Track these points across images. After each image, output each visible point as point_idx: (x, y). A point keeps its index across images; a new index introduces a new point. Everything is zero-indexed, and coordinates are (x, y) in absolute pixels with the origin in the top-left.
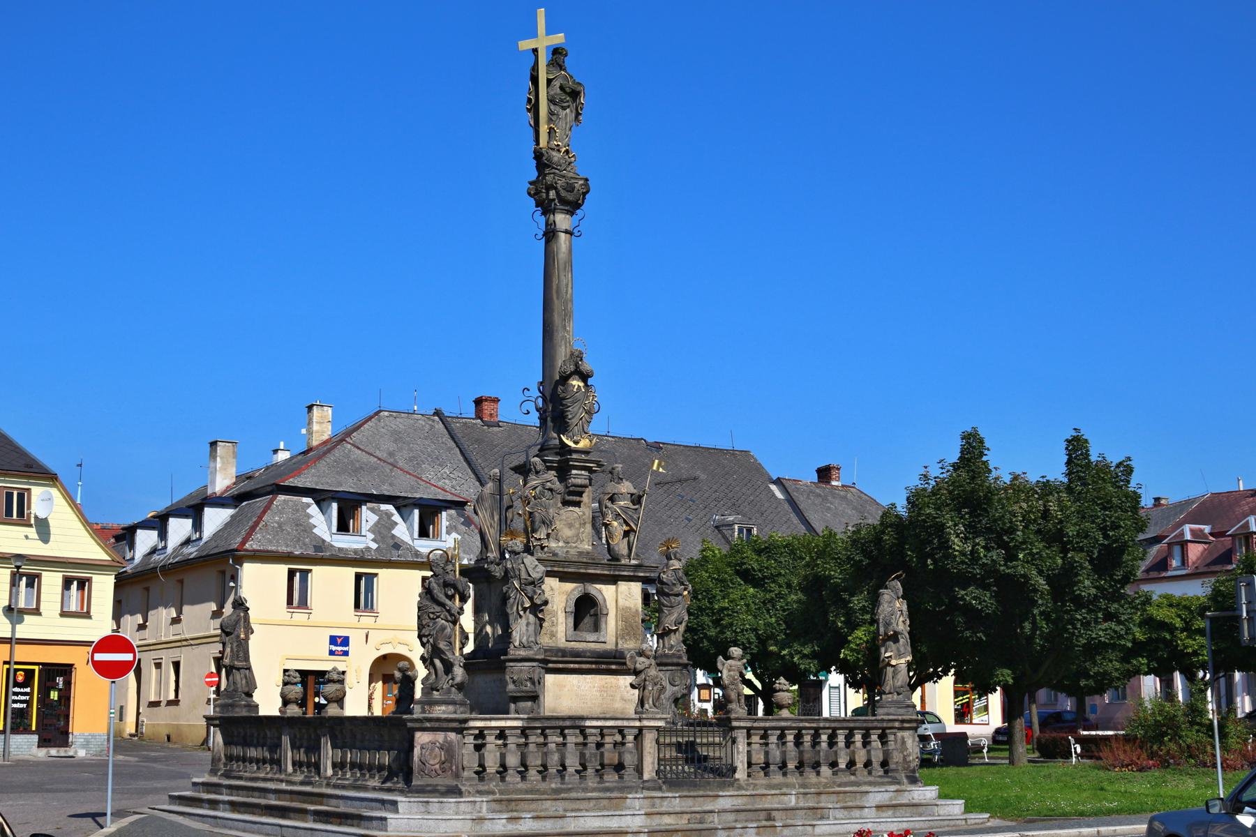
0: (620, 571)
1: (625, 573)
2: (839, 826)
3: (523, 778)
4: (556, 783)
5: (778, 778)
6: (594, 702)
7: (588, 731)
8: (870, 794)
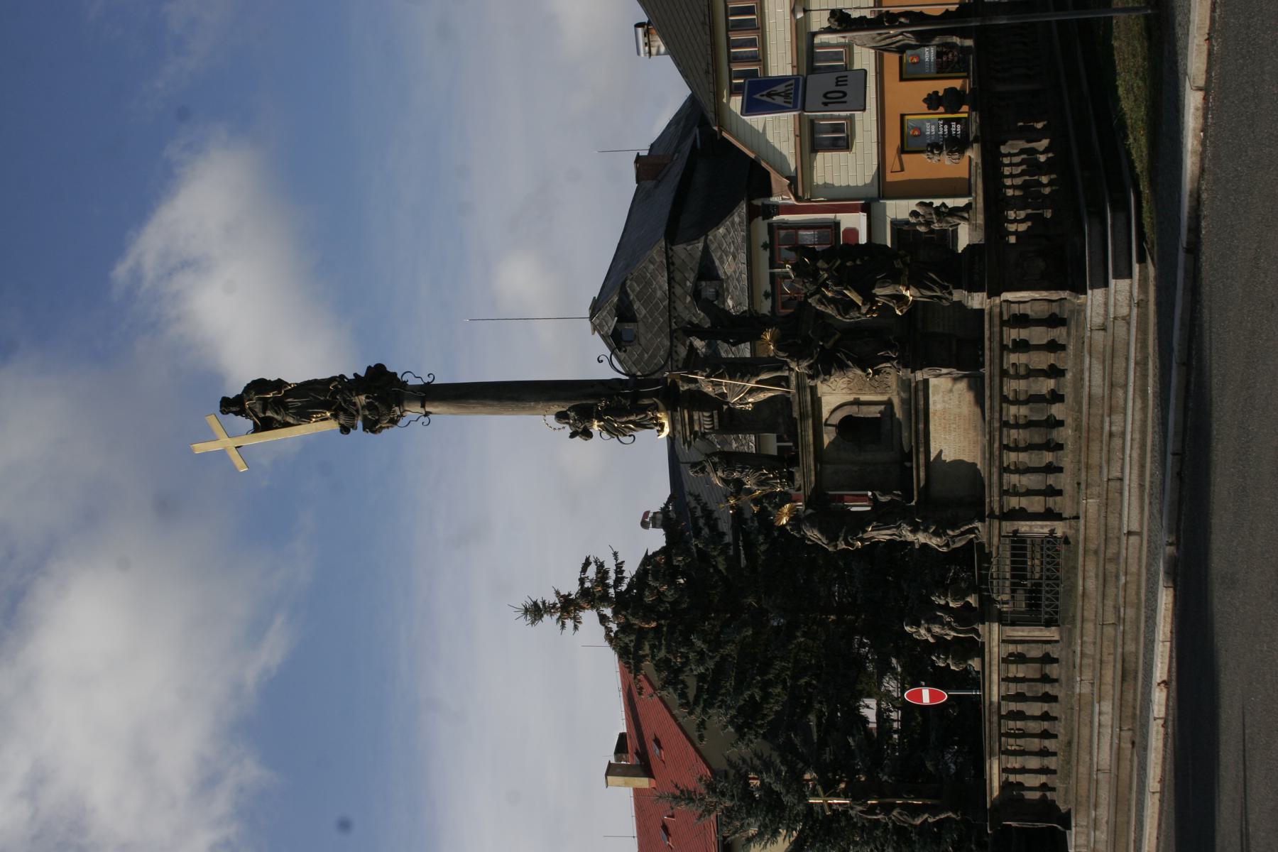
0: (806, 406)
1: (809, 398)
2: (1133, 498)
3: (1054, 754)
4: (1059, 726)
5: (1064, 481)
6: (962, 439)
7: (1003, 693)
8: (1093, 392)
